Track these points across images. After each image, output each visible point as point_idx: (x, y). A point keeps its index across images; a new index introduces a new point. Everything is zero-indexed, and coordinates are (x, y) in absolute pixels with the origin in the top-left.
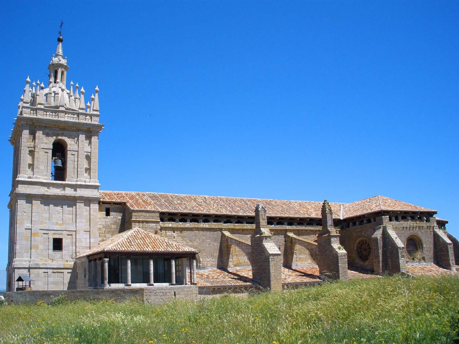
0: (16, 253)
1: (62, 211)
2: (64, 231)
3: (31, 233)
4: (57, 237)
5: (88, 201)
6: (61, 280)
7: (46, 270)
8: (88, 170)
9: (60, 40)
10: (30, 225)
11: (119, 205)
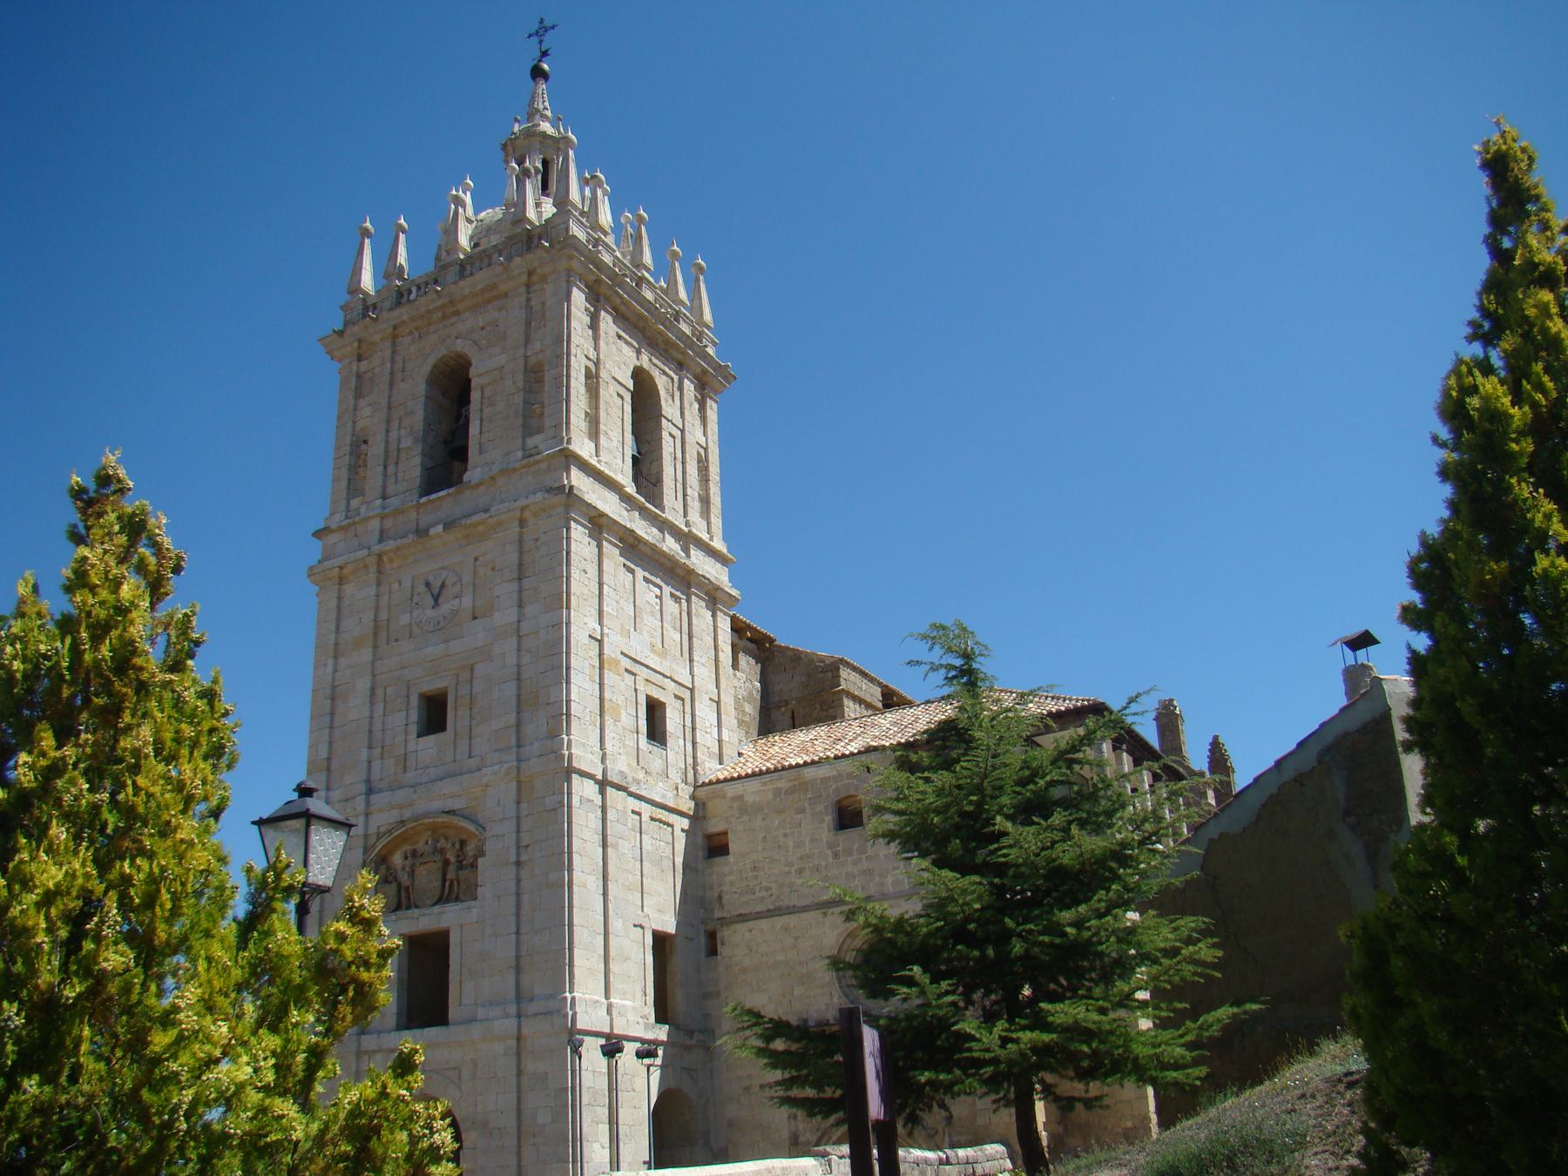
0: (568, 715)
1: (658, 608)
2: (667, 677)
3: (601, 655)
4: (657, 694)
5: (714, 598)
6: (668, 851)
7: (634, 804)
8: (705, 501)
9: (537, 73)
10: (598, 628)
11: (753, 645)
